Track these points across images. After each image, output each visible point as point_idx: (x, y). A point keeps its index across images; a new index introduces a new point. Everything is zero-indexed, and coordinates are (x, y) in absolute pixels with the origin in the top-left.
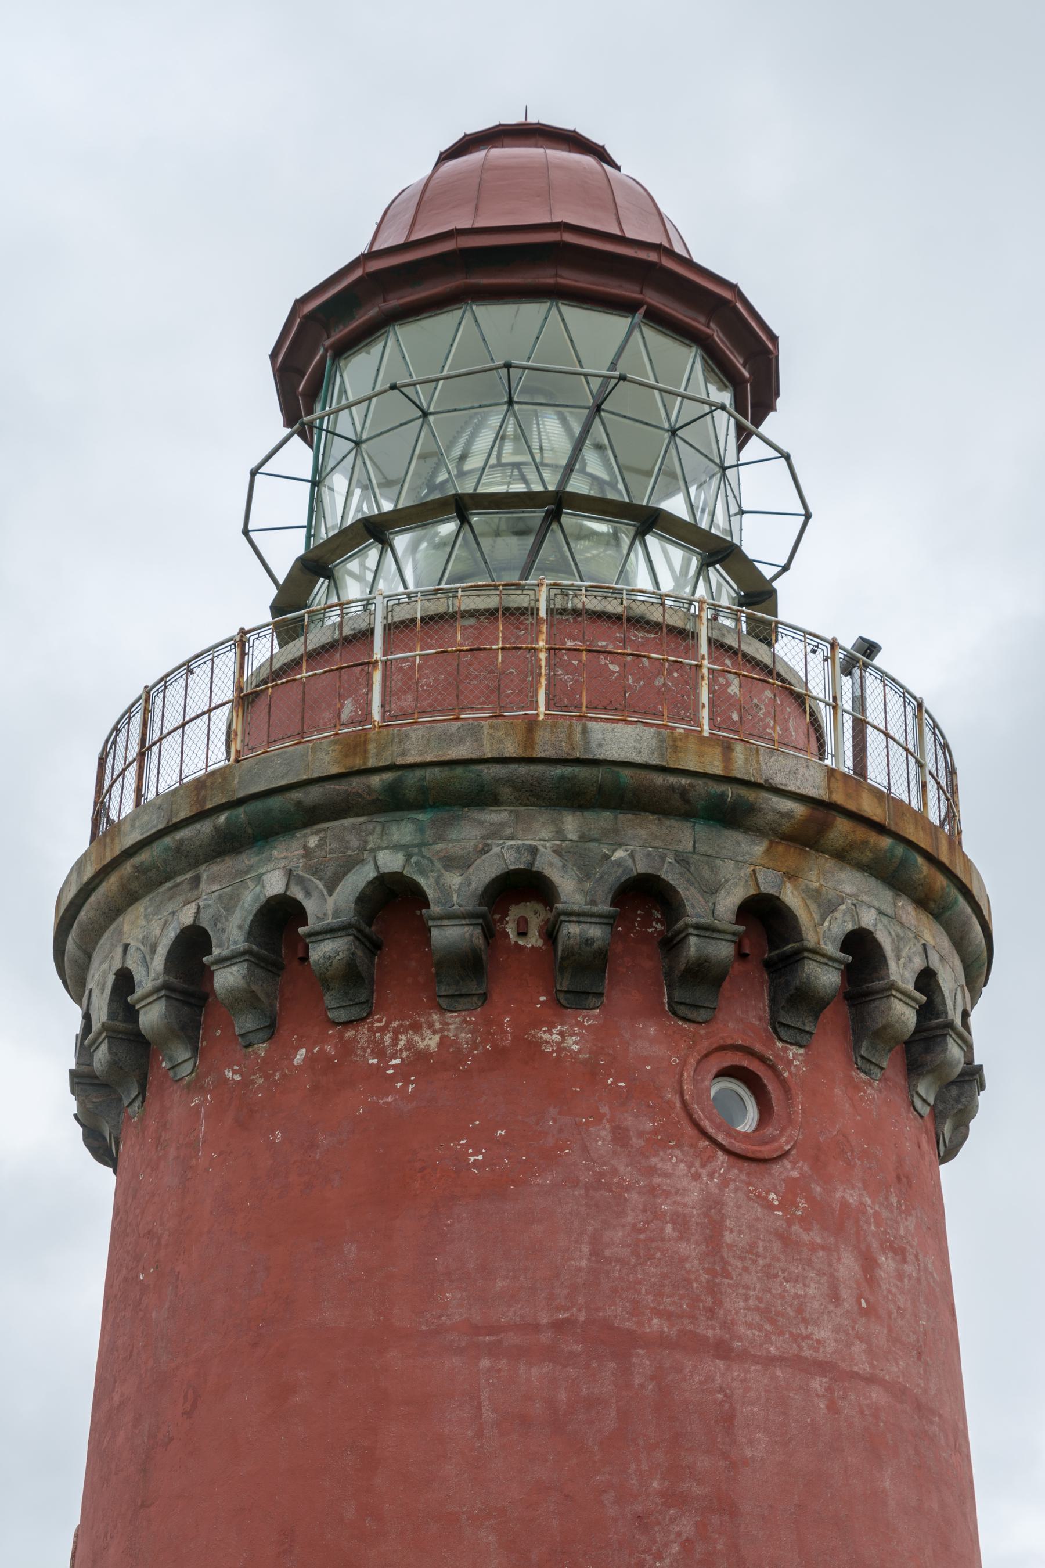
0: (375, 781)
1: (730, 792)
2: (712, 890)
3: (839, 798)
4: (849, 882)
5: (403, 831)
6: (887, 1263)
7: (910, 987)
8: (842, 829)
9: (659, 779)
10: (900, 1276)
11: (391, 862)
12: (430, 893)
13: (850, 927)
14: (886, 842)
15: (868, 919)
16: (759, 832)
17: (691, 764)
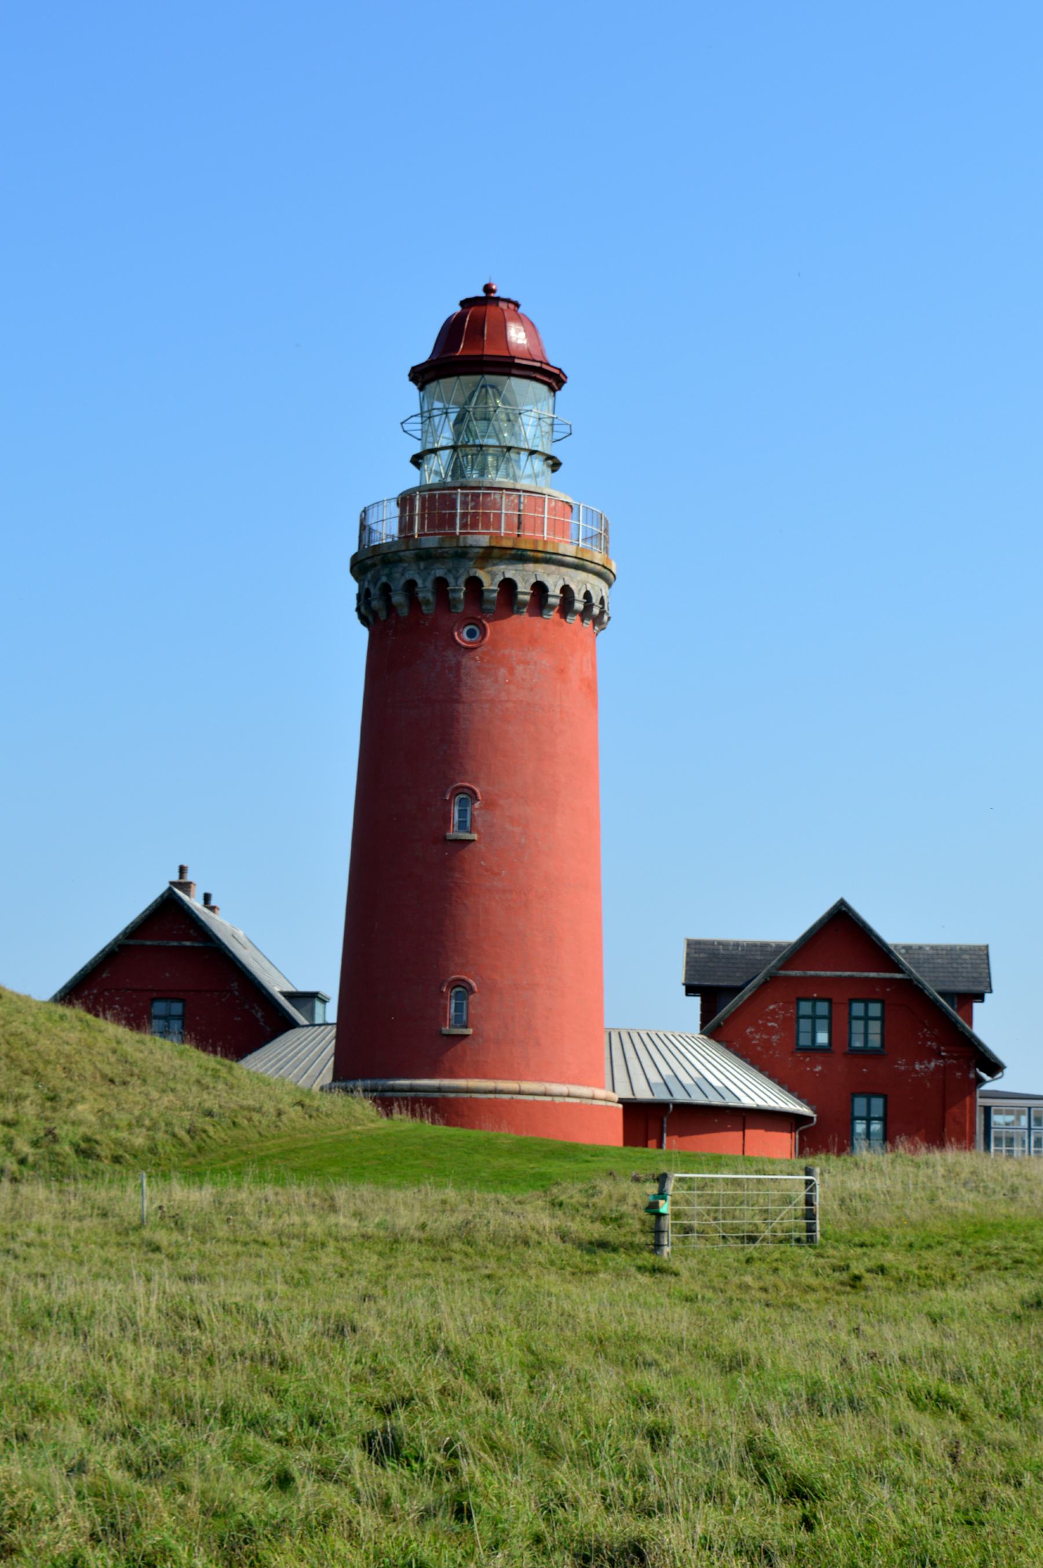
0: (379, 557)
1: (460, 550)
2: (456, 579)
3: (493, 544)
4: (502, 567)
5: (386, 571)
6: (519, 669)
7: (528, 590)
8: (496, 552)
9: (440, 551)
10: (525, 670)
11: (384, 579)
12: (393, 588)
13: (502, 578)
14: (513, 552)
15: (508, 575)
16: (471, 559)
17: (447, 544)
